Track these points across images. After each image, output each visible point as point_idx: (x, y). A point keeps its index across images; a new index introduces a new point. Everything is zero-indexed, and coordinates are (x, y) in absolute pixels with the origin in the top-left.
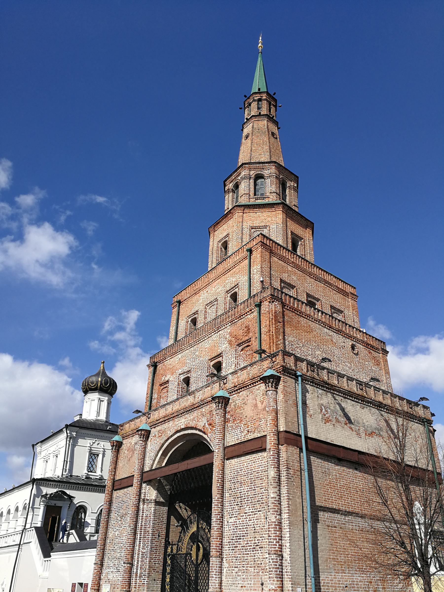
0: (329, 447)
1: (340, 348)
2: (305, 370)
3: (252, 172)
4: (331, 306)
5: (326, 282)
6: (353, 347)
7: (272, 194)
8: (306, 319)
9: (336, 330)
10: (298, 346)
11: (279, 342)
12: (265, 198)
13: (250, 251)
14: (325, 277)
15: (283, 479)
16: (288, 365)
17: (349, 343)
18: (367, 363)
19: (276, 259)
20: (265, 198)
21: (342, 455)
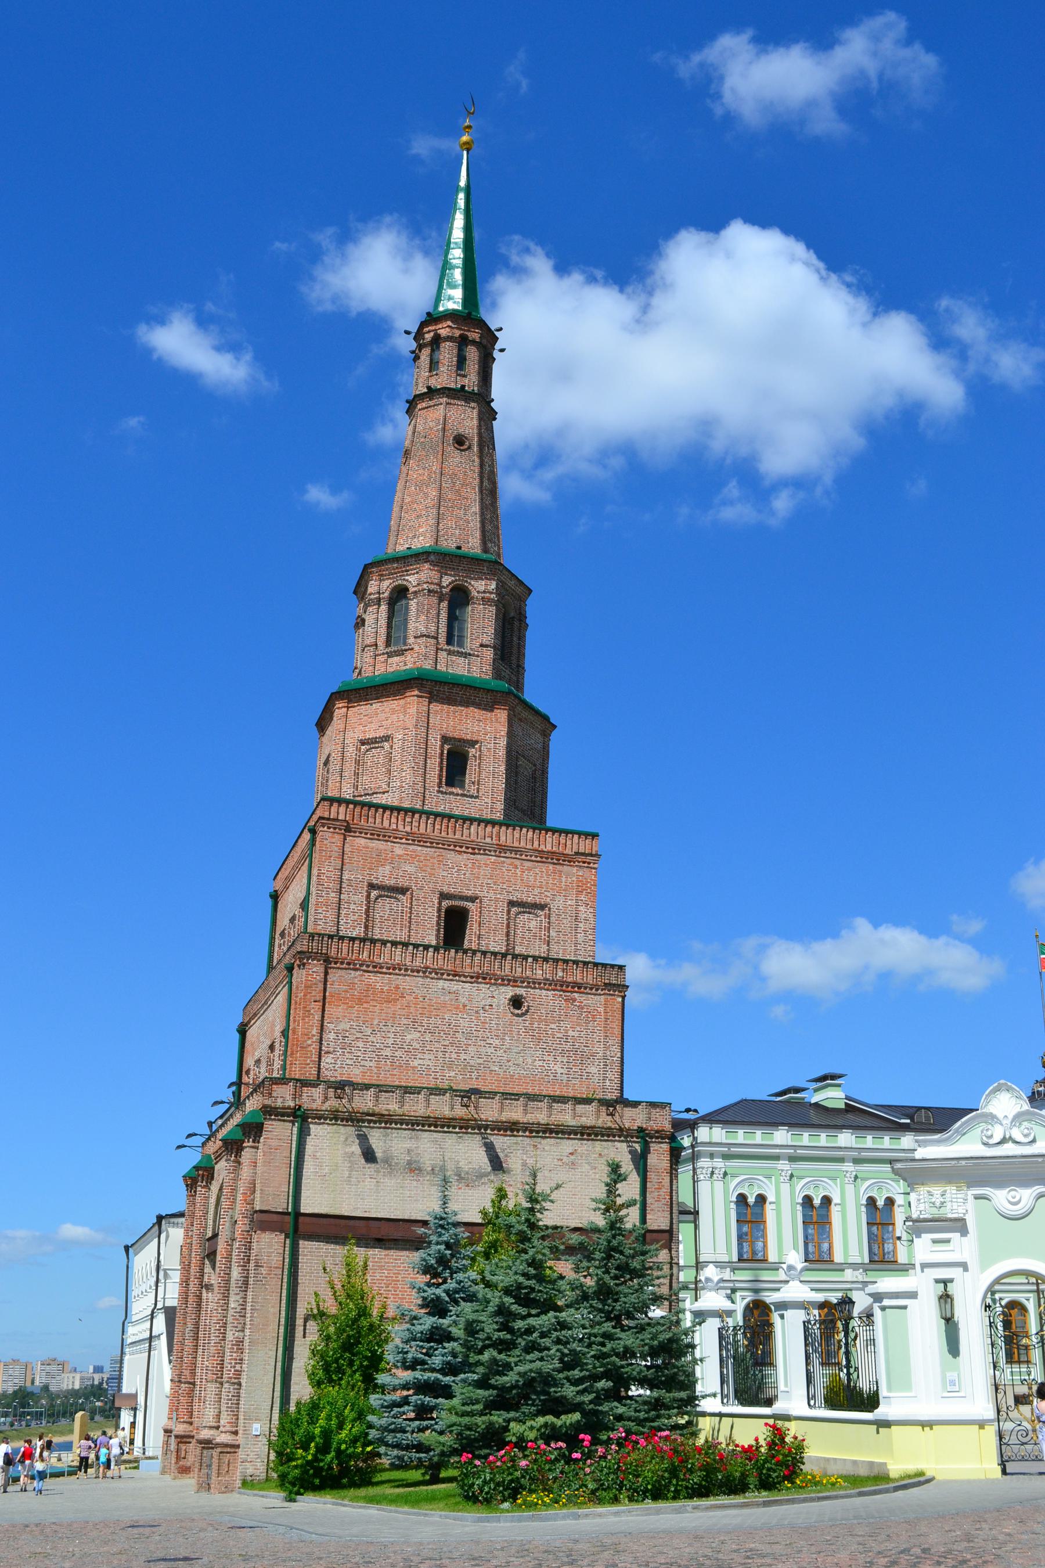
0: (352, 1223)
1: (477, 1012)
2: (319, 1102)
3: (386, 584)
4: (512, 903)
5: (502, 849)
6: (516, 1002)
7: (418, 641)
8: (390, 974)
9: (472, 977)
10: (359, 1035)
11: (309, 1042)
12: (406, 650)
13: (313, 832)
14: (503, 838)
15: (251, 1281)
16: (279, 1100)
17: (509, 992)
18: (553, 1026)
19: (363, 841)
20: (406, 650)
21: (385, 1231)
